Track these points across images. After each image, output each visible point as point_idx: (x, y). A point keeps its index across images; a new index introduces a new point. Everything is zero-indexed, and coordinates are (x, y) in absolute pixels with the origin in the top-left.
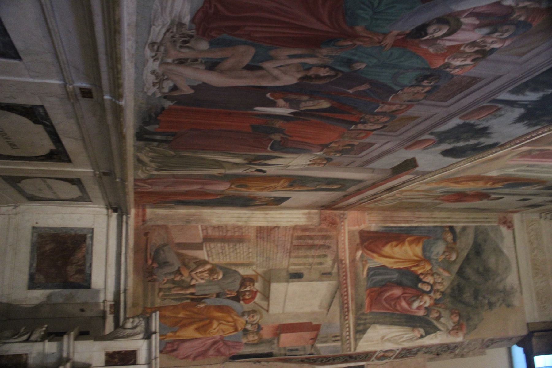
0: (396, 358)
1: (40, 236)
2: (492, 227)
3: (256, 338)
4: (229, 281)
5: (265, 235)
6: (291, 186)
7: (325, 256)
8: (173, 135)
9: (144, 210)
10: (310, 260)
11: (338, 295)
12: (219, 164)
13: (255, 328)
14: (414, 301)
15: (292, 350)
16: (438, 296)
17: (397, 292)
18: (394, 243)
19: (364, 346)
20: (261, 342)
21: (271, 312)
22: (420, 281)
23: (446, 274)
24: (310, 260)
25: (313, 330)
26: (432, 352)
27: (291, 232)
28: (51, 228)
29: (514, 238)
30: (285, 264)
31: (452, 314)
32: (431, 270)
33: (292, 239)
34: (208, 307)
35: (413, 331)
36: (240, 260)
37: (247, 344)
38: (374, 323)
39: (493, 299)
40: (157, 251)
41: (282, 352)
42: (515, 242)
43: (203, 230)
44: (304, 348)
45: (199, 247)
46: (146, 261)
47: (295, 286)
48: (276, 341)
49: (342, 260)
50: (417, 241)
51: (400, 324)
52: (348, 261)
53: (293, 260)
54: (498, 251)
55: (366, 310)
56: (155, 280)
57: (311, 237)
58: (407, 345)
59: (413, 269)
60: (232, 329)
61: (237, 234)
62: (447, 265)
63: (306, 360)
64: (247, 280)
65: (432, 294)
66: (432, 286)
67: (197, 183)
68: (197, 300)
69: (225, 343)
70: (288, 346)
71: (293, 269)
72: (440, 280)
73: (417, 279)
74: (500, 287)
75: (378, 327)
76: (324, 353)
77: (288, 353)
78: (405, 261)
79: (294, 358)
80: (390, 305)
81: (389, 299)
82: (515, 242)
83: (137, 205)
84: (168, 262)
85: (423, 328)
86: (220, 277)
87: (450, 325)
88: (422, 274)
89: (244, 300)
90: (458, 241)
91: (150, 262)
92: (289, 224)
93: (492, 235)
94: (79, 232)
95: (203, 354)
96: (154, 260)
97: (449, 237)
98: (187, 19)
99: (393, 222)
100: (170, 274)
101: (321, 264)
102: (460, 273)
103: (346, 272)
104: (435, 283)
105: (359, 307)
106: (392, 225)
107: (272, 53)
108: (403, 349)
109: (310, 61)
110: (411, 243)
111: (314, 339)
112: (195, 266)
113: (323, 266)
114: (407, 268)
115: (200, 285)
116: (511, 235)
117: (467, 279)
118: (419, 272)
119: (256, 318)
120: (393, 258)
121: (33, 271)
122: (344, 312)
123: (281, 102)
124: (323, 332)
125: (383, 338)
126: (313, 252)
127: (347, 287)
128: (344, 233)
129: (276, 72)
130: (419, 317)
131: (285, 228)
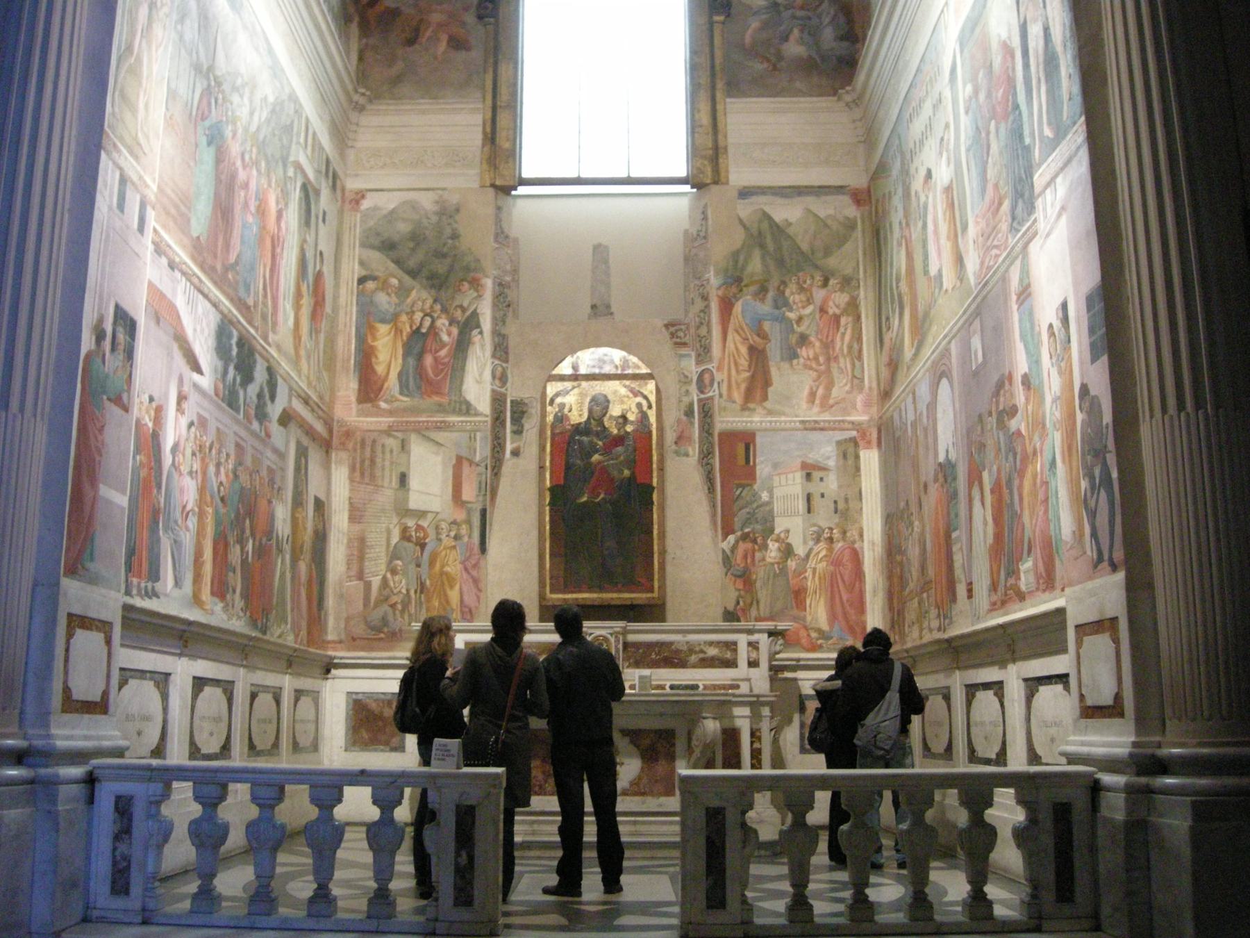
0: (507, 361)
1: (354, 743)
2: (362, 221)
3: (464, 526)
4: (404, 553)
5: (359, 513)
6: (301, 504)
7: (383, 446)
8: (263, 610)
9: (329, 642)
10: (387, 463)
11: (427, 433)
12: (283, 574)
13: (454, 527)
14: (441, 340)
15: (480, 488)
16: (438, 307)
17: (428, 360)
18: (374, 360)
19: (483, 405)
20: (468, 522)
21: (438, 510)
22: (419, 328)
23: (414, 293)
24: (387, 463)
26: (505, 315)
27: (355, 484)
28: (346, 733)
31: (460, 290)
32: (407, 314)
33: (362, 483)
34: (430, 577)
35: (474, 344)
36: (384, 542)
37: (470, 537)
38: (460, 391)
39: (448, 231)
40: (372, 628)
41: (481, 498)
42: (382, 190)
44: (480, 474)
45: (368, 586)
46: (382, 639)
47: (414, 483)
48: (469, 505)
49: (389, 427)
50: (372, 329)
51: (465, 359)
53: (386, 484)
54: (392, 216)
55: (445, 400)
56: (400, 630)
57: (363, 461)
58: (488, 352)
59: (405, 338)
60: (454, 552)
61: (356, 544)
62: (403, 291)
65: (435, 315)
66: (426, 315)
67: (299, 590)
68: (422, 588)
69: (467, 559)
70: (475, 492)
71: (395, 483)
72: (420, 303)
73: (416, 332)
74: (434, 219)
75: (464, 387)
76: (488, 452)
77: (483, 493)
79: (491, 485)
80: (442, 370)
82: (382, 190)
83: (326, 649)
84: (383, 618)
85: (471, 331)
86: (399, 562)
88: (411, 327)
89: (425, 538)
90: (377, 274)
91: (382, 635)
92: (347, 485)
93: (371, 223)
94: (351, 707)
95: (476, 581)
96: (380, 631)
97: (370, 285)
99: (349, 360)
100: (395, 614)
101: (391, 451)
102: (413, 274)
103: (402, 422)
104: (422, 310)
105: (441, 409)
106: (352, 362)
108: (494, 356)
110: (374, 338)
111: (471, 462)
112: (388, 589)
113: (395, 449)
114: (403, 346)
115: (408, 584)
116: (372, 193)
117: (421, 266)
118: (409, 330)
119: (444, 525)
120: (390, 362)
121: (388, 749)
122: (443, 427)
124: (464, 453)
125: (478, 382)
126: (379, 460)
127: (419, 422)
128: (359, 422)
130: (461, 333)
131: (351, 490)
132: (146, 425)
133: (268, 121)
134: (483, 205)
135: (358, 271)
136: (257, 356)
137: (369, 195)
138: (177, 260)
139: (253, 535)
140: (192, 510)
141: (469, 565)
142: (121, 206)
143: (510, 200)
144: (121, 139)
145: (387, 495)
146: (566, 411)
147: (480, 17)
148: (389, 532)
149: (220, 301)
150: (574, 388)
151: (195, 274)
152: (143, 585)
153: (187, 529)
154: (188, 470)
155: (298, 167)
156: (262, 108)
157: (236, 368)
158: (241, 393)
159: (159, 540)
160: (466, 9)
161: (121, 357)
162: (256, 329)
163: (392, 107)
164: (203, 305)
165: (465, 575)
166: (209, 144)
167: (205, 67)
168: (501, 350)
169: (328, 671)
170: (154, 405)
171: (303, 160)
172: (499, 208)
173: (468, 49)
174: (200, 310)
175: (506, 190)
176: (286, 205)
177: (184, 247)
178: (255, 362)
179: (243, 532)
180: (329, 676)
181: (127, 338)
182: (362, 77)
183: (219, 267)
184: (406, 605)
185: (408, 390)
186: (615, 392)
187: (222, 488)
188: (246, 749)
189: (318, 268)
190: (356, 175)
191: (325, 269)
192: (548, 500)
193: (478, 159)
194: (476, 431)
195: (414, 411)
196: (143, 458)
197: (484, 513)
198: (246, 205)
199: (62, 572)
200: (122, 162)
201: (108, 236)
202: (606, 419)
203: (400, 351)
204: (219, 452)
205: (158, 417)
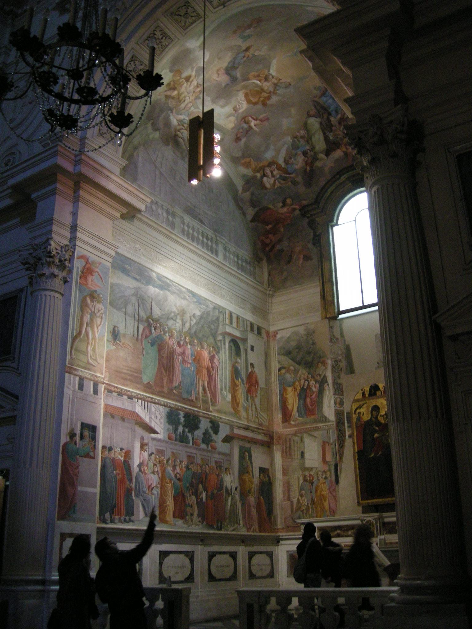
0: (343, 395)
7: (294, 440)
9: (278, 529)
10: (296, 448)
12: (233, 504)
14: (312, 390)
15: (333, 455)
16: (310, 376)
17: (308, 400)
18: (287, 403)
20: (330, 470)
23: (300, 372)
24: (296, 448)
25: (325, 445)
29: (282, 329)
30: (298, 461)
37: (331, 477)
39: (311, 342)
41: (334, 459)
43: (285, 501)
44: (332, 449)
45: (292, 503)
47: (307, 456)
48: (329, 463)
51: (322, 397)
52: (296, 429)
53: (296, 457)
57: (286, 448)
58: (332, 392)
62: (296, 371)
63: (341, 445)
64: (305, 480)
65: (309, 380)
66: (306, 380)
68: (313, 502)
69: (331, 487)
71: (299, 457)
72: (303, 376)
73: (302, 389)
74: (305, 337)
75: (324, 410)
77: (335, 456)
78: (295, 397)
81: (312, 405)
83: (277, 532)
85: (324, 384)
86: (303, 492)
87: (323, 368)
88: (300, 387)
89: (313, 480)
90: (286, 366)
92: (281, 460)
93: (281, 344)
97: (283, 371)
98: (183, 521)
101: (297, 443)
102: (299, 363)
103: (300, 429)
105: (315, 421)
107: (187, 504)
108: (334, 394)
109: (188, 496)
110: (287, 394)
111: (329, 444)
115: (308, 501)
116: (281, 331)
118: (299, 388)
119: (320, 473)
122: (317, 429)
123: (201, 496)
124: (326, 440)
126: (292, 447)
127: (307, 428)
129: (192, 501)
131: (283, 462)
132: (120, 459)
133: (197, 323)
134: (323, 327)
135: (278, 366)
136: (201, 418)
137: (279, 332)
138: (134, 394)
139: (205, 489)
140: (156, 486)
141: (331, 490)
142: (81, 387)
143: (338, 323)
144: (78, 366)
145: (296, 462)
146: (361, 415)
147: (314, 244)
148: (299, 478)
149: (167, 403)
150: (364, 404)
151: (147, 397)
152: (122, 518)
153: (152, 494)
154: (150, 471)
155: (225, 334)
156: (191, 320)
157: (184, 426)
158: (190, 436)
159: (132, 500)
160: (309, 242)
161: (88, 440)
162: (199, 408)
163: (284, 292)
164: (153, 407)
165: (330, 495)
166: (152, 345)
167: (145, 317)
168: (339, 390)
169: (278, 542)
170: (124, 451)
171: (229, 330)
172: (331, 327)
173: (312, 259)
174: (153, 409)
175: (335, 318)
176: (218, 352)
177: (138, 389)
178: (199, 421)
179: (197, 490)
180: (279, 544)
181: (91, 433)
182: (271, 283)
183: (165, 390)
184: (307, 510)
185: (301, 414)
186: (382, 403)
187: (178, 475)
188: (206, 578)
189: (250, 370)
190: (274, 325)
191: (256, 370)
192: (357, 457)
193: (320, 308)
194: (329, 429)
195: (305, 423)
196: (118, 471)
197: (336, 466)
198: (184, 361)
199: (56, 519)
200: (80, 373)
201: (73, 401)
202: (379, 417)
203: (297, 398)
204: (175, 461)
205: (128, 454)
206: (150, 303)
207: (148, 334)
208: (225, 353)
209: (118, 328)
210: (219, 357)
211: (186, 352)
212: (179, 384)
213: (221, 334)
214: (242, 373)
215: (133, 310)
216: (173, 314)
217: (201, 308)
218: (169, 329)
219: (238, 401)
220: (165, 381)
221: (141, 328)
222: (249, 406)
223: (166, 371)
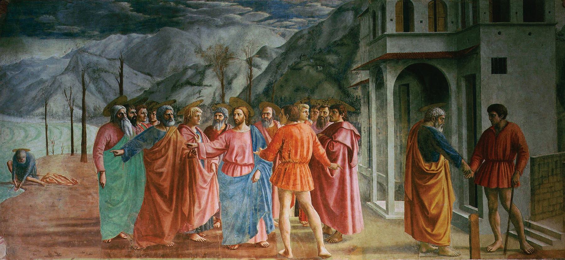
133: (275, 67)
167: (103, 105)
183: (169, 241)
189: (486, 124)
206: (117, 72)
207: (114, 138)
208: (382, 106)
209: (26, 151)
210: (357, 125)
211: (236, 144)
212: (211, 220)
213: (364, 67)
214: (454, 141)
215: (67, 103)
216: (190, 73)
217: (286, 27)
218: (177, 109)
219: (433, 211)
220: (167, 223)
221: (92, 131)
222: (481, 215)
223: (169, 201)
